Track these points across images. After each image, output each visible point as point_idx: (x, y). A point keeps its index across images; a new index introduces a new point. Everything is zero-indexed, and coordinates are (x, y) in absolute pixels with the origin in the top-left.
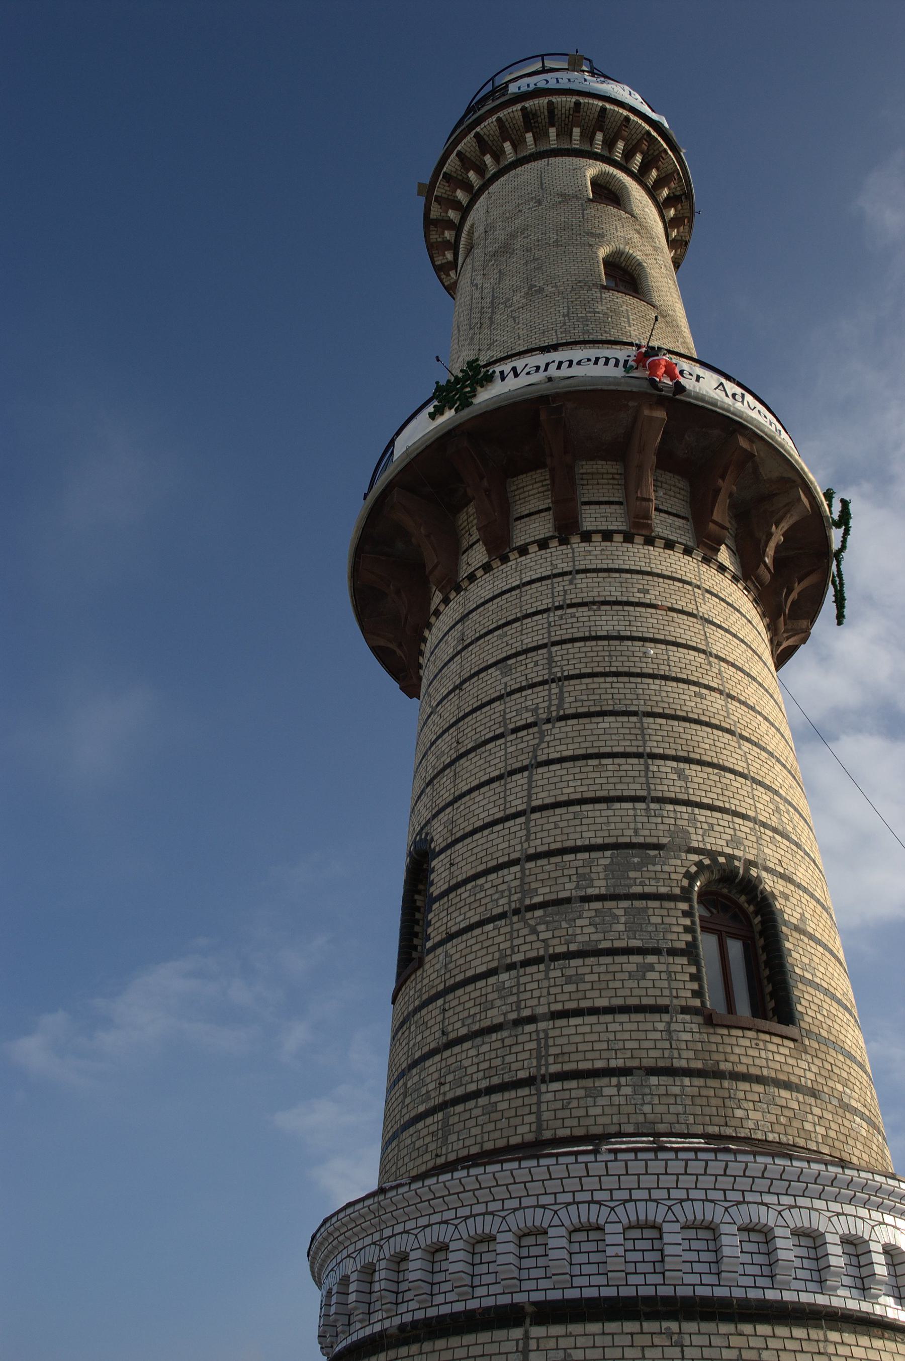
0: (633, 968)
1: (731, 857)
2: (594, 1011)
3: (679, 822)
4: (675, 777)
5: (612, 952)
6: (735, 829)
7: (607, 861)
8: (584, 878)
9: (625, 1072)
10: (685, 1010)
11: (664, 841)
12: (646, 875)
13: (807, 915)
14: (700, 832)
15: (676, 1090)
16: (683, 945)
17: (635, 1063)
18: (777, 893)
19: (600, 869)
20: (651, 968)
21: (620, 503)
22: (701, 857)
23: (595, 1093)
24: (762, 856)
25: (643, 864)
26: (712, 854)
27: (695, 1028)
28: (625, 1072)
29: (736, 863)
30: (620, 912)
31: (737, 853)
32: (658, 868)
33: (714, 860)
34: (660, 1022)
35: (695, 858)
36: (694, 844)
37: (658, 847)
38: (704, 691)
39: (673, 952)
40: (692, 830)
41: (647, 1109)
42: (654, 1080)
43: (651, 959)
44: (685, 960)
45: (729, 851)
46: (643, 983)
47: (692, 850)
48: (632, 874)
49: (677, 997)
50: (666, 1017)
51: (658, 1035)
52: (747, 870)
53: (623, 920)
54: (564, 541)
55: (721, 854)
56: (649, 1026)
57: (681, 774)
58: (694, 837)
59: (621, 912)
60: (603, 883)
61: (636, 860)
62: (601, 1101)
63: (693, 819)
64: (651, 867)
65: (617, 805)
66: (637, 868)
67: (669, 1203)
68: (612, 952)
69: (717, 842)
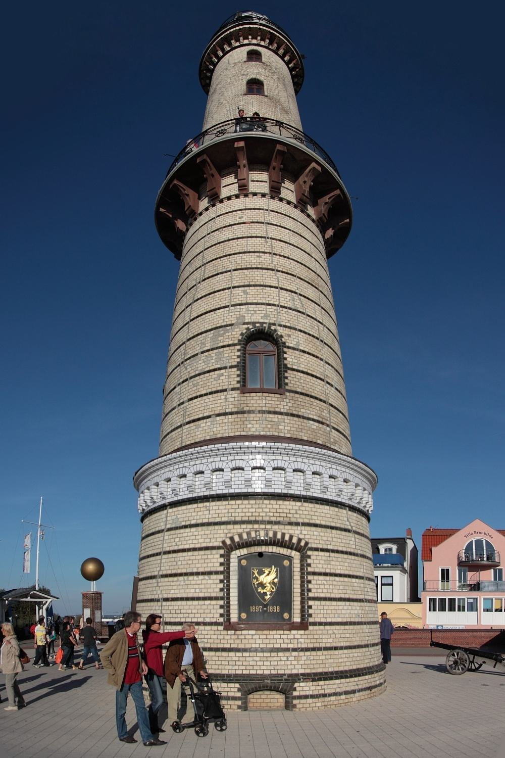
0: (216, 376)
2: (201, 396)
3: (241, 313)
4: (242, 294)
6: (266, 311)
7: (211, 335)
9: (209, 417)
10: (233, 389)
11: (233, 322)
12: (225, 337)
13: (300, 342)
14: (250, 315)
15: (226, 421)
16: (235, 363)
17: (212, 413)
18: (283, 334)
19: (209, 339)
22: (249, 326)
24: (279, 320)
25: (224, 334)
26: (254, 323)
27: (236, 395)
28: (209, 417)
29: (265, 325)
30: (214, 355)
31: (265, 321)
32: (230, 334)
34: (222, 395)
35: (246, 326)
36: (246, 321)
37: (231, 325)
40: (246, 315)
41: (215, 429)
42: (218, 418)
43: (223, 371)
44: (235, 369)
45: (262, 321)
46: (219, 382)
47: (244, 324)
48: (220, 339)
49: (231, 385)
51: (221, 401)
52: (269, 327)
53: (214, 358)
55: (258, 323)
56: (219, 398)
57: (245, 292)
58: (246, 318)
59: (214, 355)
60: (209, 344)
61: (222, 332)
62: (200, 429)
64: (227, 334)
65: (218, 311)
67: (269, 460)
69: (258, 318)
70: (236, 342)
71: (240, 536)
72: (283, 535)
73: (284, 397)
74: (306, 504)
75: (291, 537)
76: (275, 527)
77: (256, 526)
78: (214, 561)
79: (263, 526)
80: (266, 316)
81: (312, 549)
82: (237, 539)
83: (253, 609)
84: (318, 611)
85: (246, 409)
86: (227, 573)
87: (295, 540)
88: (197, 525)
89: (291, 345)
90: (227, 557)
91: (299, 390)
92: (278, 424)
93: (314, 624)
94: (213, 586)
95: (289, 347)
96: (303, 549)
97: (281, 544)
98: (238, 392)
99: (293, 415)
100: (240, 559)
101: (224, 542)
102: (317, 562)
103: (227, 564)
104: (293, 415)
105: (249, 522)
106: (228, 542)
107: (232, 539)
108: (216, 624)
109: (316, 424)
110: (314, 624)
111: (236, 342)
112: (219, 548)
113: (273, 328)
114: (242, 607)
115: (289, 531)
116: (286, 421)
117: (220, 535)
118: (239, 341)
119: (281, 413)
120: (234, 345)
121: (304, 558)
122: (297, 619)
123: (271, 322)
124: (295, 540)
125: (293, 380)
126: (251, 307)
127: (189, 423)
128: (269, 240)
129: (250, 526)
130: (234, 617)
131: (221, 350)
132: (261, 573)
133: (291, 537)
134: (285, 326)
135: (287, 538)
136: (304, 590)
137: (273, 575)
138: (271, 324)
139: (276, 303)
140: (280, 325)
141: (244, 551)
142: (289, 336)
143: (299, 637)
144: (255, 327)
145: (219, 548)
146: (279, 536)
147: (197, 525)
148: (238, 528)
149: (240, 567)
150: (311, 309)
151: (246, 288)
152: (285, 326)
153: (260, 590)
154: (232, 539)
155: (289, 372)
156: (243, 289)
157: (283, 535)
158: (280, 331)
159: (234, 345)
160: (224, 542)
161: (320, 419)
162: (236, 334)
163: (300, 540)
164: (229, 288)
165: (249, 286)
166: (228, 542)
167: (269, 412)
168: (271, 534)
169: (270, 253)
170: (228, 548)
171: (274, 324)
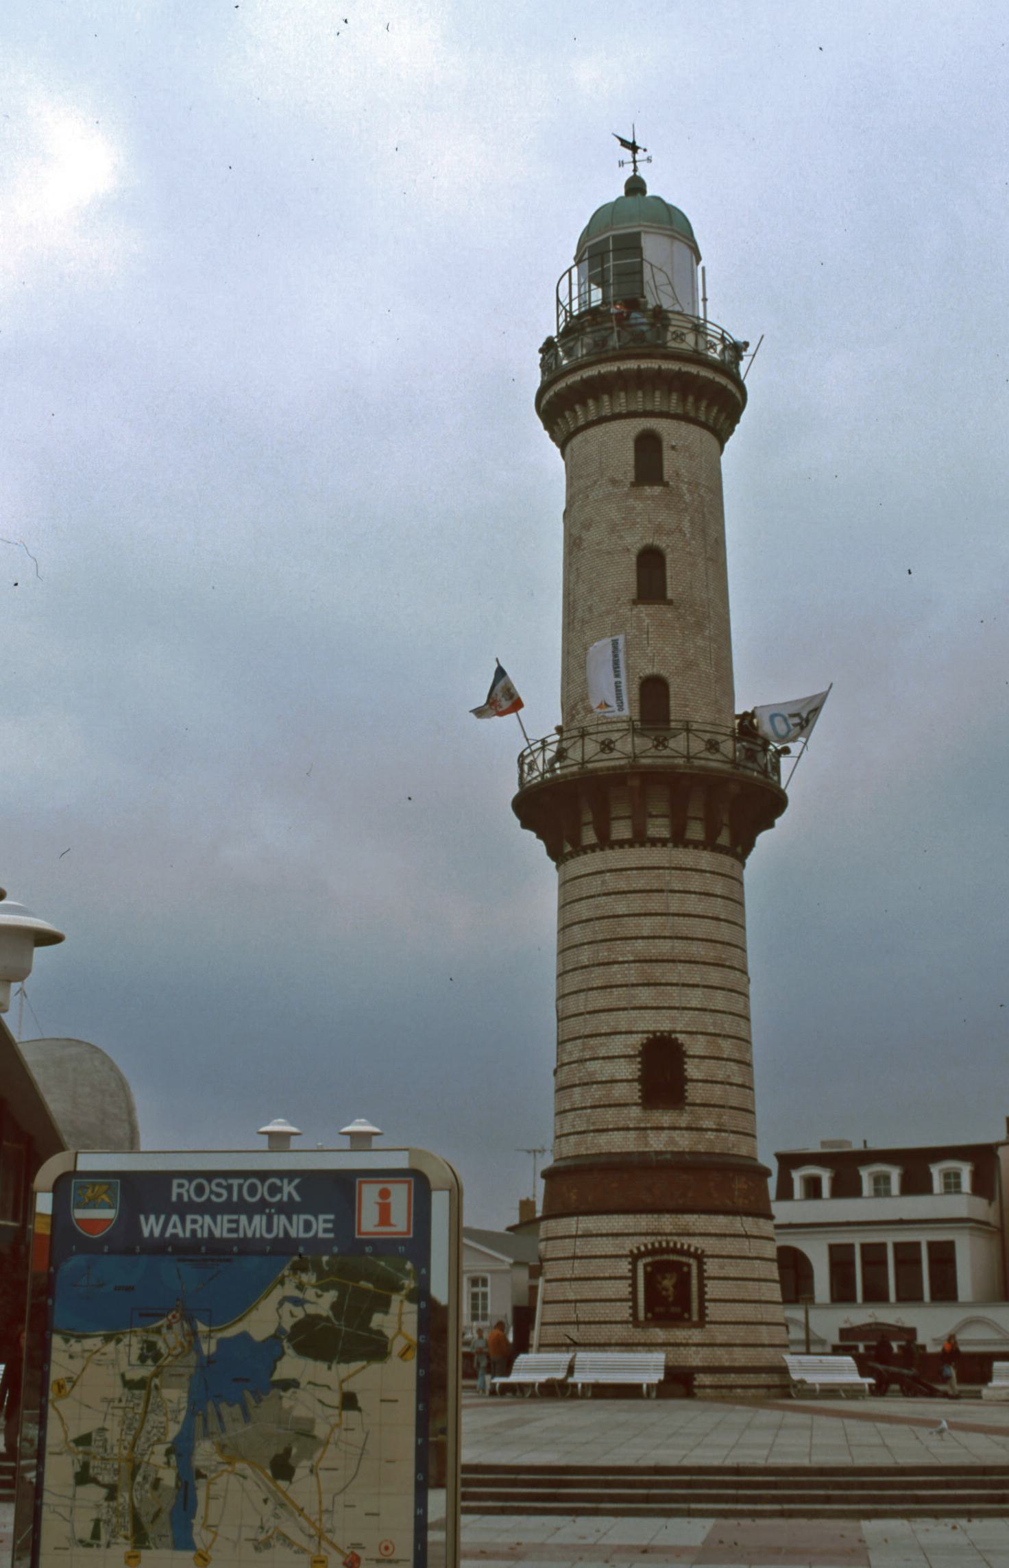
1: (662, 1032)
21: (629, 817)
26: (654, 1033)
54: (602, 849)
71: (646, 1246)
72: (682, 1245)
75: (689, 1246)
76: (675, 1238)
77: (659, 1238)
78: (624, 1267)
81: (708, 1257)
82: (643, 1248)
83: (657, 1310)
84: (713, 1311)
86: (634, 1278)
87: (692, 1249)
88: (607, 1235)
90: (634, 1264)
93: (711, 1323)
94: (623, 1288)
95: (690, 1057)
96: (700, 1257)
97: (682, 1252)
100: (645, 1266)
101: (631, 1251)
102: (711, 1267)
103: (634, 1271)
105: (653, 1234)
106: (635, 1251)
107: (638, 1249)
108: (626, 1322)
110: (711, 1323)
112: (626, 1256)
113: (673, 1036)
114: (648, 1308)
115: (686, 1241)
117: (630, 1245)
121: (701, 1264)
122: (695, 1318)
124: (692, 1249)
125: (694, 1093)
129: (654, 1238)
130: (641, 1315)
132: (664, 1278)
133: (689, 1246)
135: (686, 1247)
136: (702, 1293)
137: (673, 1281)
141: (649, 1260)
143: (696, 1335)
145: (626, 1256)
146: (679, 1246)
147: (607, 1235)
148: (644, 1239)
149: (646, 1273)
153: (664, 1293)
154: (638, 1249)
157: (682, 1245)
158: (681, 1038)
160: (631, 1251)
163: (696, 1249)
166: (635, 1251)
168: (671, 1245)
170: (635, 1257)
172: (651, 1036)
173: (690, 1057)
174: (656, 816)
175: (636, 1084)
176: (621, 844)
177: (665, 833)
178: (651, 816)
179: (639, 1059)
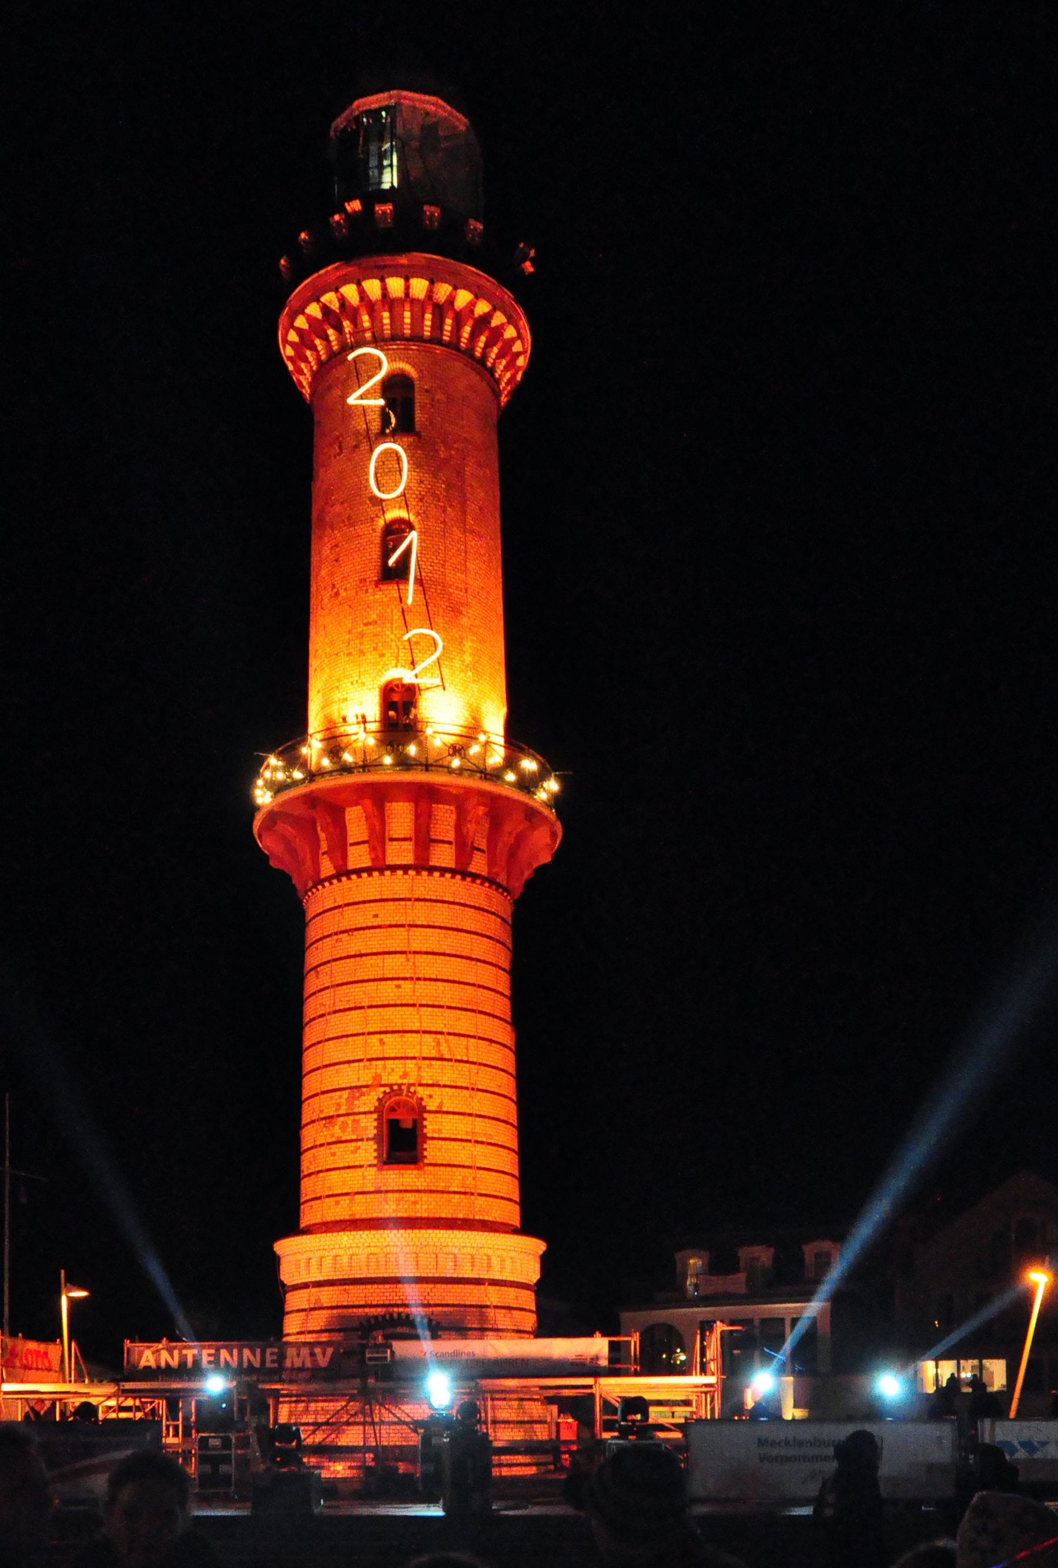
1: (400, 1085)
5: (346, 1141)
8: (339, 1105)
10: (370, 1166)
20: (359, 1148)
23: (337, 1203)
26: (391, 1086)
33: (391, 1088)
35: (382, 1089)
36: (383, 1082)
37: (367, 1086)
38: (401, 982)
39: (368, 1139)
43: (359, 1144)
45: (400, 1082)
50: (363, 1169)
57: (382, 1042)
63: (384, 1067)
66: (358, 1098)
68: (346, 1141)
69: (394, 1079)
70: (373, 1109)
73: (421, 1172)
74: (438, 1286)
79: (396, 1310)
80: (405, 1075)
85: (383, 1189)
89: (433, 1108)
91: (439, 1162)
92: (415, 1203)
95: (430, 1112)
98: (375, 1169)
99: (431, 1191)
104: (431, 1191)
109: (457, 1196)
111: (373, 1109)
113: (412, 1089)
116: (424, 1199)
118: (376, 1108)
119: (418, 1191)
120: (371, 1112)
123: (412, 1081)
125: (432, 1151)
126: (389, 1064)
127: (328, 1196)
128: (411, 956)
131: (357, 1117)
134: (428, 1085)
138: (410, 1085)
139: (417, 1055)
140: (421, 1085)
142: (431, 1096)
144: (391, 1088)
150: (459, 1048)
151: (383, 1036)
152: (428, 1085)
155: (429, 1142)
156: (378, 1036)
158: (421, 1092)
159: (371, 1112)
161: (462, 1190)
162: (369, 1101)
164: (363, 1034)
165: (386, 1032)
167: (407, 1191)
169: (412, 979)
171: (414, 1085)
172: (388, 1090)
173: (430, 1112)
174: (398, 840)
175: (371, 1143)
176: (358, 872)
177: (408, 859)
178: (392, 840)
179: (375, 1116)
